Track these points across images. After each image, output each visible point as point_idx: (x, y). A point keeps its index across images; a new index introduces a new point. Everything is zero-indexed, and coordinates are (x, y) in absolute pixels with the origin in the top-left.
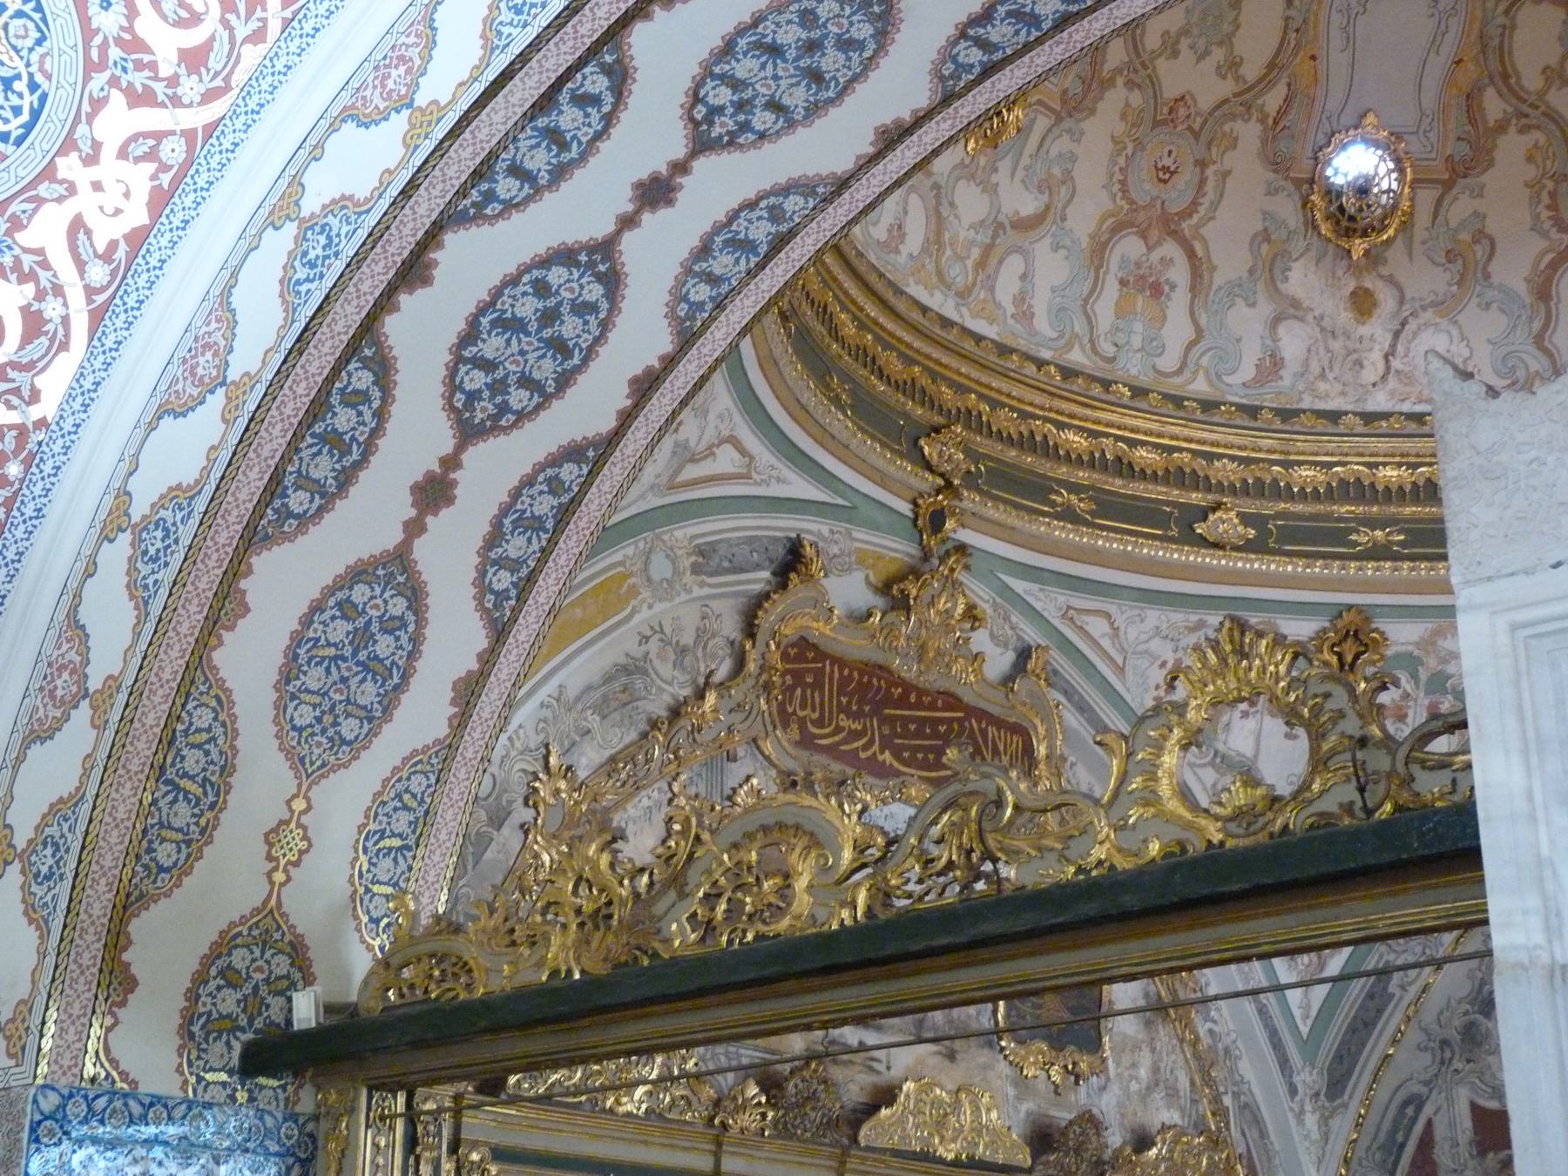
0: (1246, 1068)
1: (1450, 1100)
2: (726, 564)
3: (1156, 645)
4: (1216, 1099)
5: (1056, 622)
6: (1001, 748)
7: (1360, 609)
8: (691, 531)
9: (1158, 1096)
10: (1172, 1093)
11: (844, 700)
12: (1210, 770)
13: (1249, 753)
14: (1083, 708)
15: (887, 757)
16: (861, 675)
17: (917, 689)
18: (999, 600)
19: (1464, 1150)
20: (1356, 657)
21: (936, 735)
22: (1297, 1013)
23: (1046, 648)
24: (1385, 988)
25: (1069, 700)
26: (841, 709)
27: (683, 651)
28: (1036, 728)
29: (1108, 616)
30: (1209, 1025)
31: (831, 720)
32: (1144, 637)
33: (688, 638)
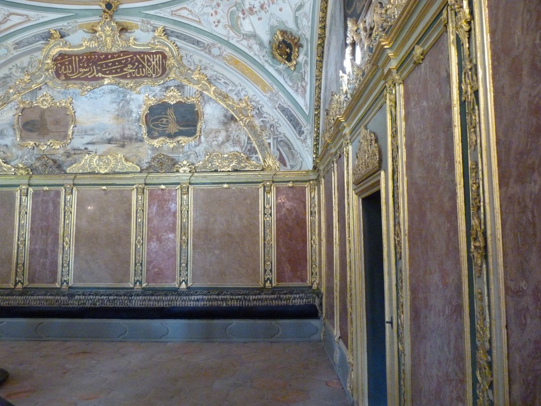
2: (27, 44)
3: (206, 10)
6: (152, 60)
8: (12, 40)
9: (227, 144)
10: (236, 142)
11: (81, 65)
12: (244, 40)
13: (252, 30)
14: (186, 38)
15: (100, 75)
16: (87, 57)
17: (110, 54)
18: (144, 19)
21: (122, 64)
22: (304, 108)
25: (179, 38)
26: (80, 67)
27: (23, 69)
28: (164, 50)
29: (186, 8)
31: (76, 71)
32: (200, 9)
33: (26, 65)
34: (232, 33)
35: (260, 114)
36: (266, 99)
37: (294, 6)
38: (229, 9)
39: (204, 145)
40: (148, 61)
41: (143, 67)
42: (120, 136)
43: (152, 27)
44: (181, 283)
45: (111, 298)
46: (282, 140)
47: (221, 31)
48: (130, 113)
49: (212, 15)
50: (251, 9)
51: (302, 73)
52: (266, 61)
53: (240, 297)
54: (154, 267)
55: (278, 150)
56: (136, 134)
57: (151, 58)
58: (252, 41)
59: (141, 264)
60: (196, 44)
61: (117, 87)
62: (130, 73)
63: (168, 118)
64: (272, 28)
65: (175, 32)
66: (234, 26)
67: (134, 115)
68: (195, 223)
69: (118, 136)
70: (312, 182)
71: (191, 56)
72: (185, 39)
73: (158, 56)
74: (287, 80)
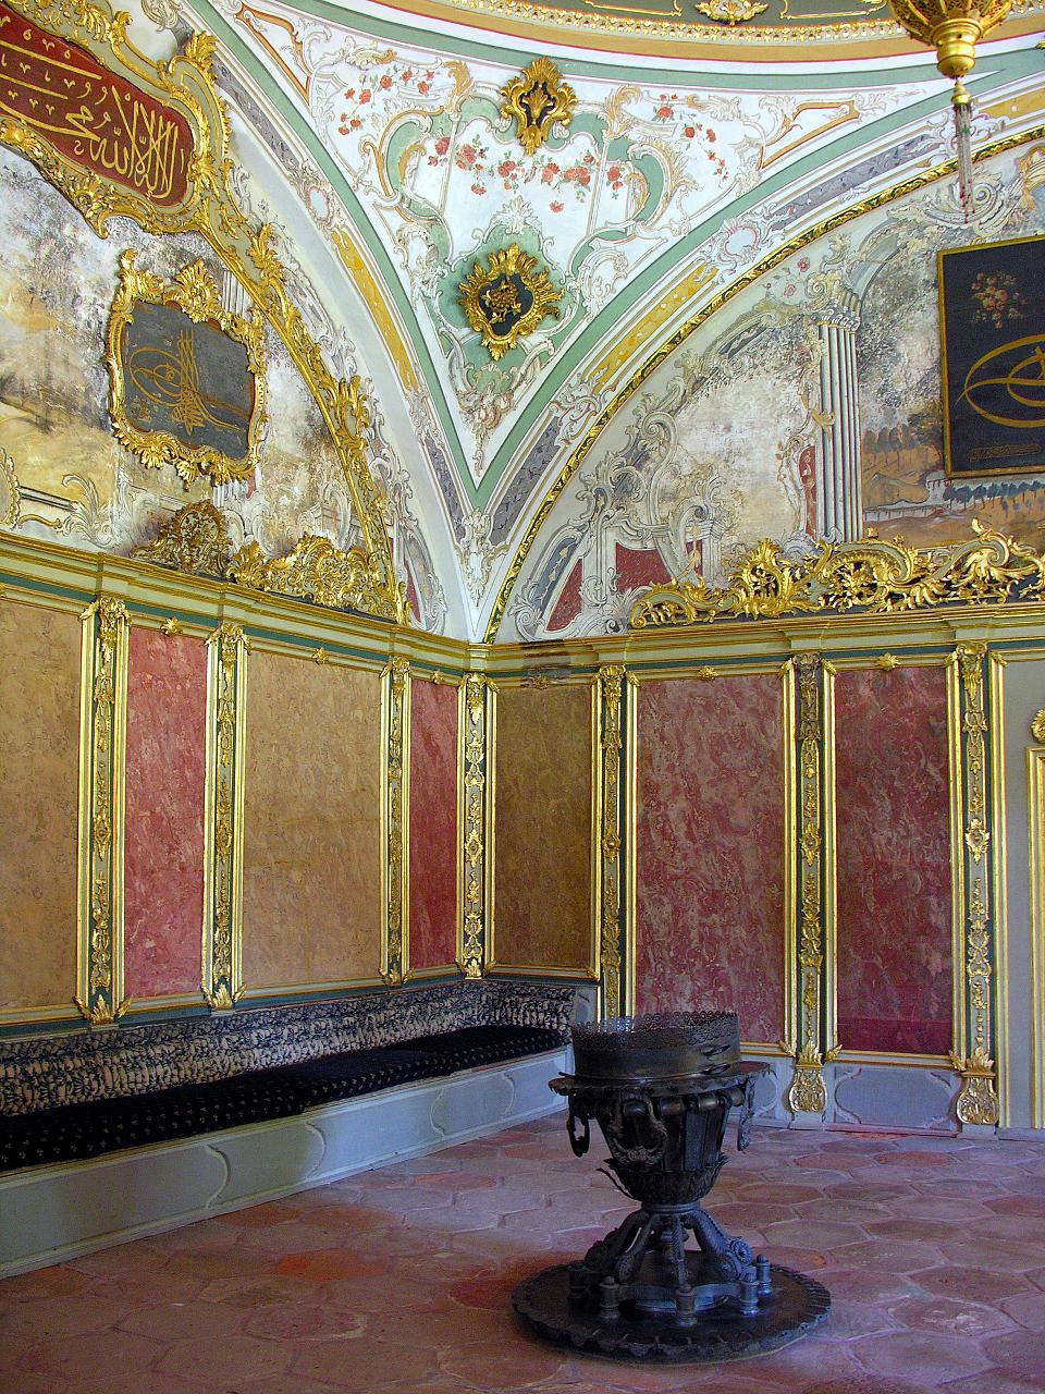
0: (414, 506)
1: (599, 543)
3: (342, 70)
4: (381, 529)
5: (230, 20)
6: (151, 131)
7: (545, 60)
9: (313, 514)
10: (331, 515)
13: (436, 203)
14: (255, 117)
19: (607, 586)
20: (544, 113)
21: (62, 89)
22: (471, 463)
23: (211, 41)
24: (552, 442)
30: (379, 460)
32: (330, 59)
34: (373, 176)
35: (377, 444)
36: (408, 407)
37: (600, 223)
38: (408, 113)
39: (263, 501)
40: (142, 131)
41: (125, 141)
42: (38, 378)
43: (175, 18)
44: (216, 988)
45: (35, 1068)
46: (412, 540)
47: (347, 150)
48: (71, 297)
49: (350, 94)
50: (469, 153)
51: (512, 377)
52: (426, 298)
53: (351, 1020)
54: (143, 935)
55: (406, 564)
56: (88, 391)
57: (149, 119)
58: (417, 228)
59: (93, 924)
60: (278, 148)
61: (35, 173)
62: (85, 141)
63: (179, 368)
64: (498, 229)
65: (231, 76)
66: (392, 161)
67: (84, 313)
68: (251, 770)
69: (28, 376)
70: (475, 678)
71: (243, 177)
72: (255, 119)
73: (169, 127)
74: (457, 372)
